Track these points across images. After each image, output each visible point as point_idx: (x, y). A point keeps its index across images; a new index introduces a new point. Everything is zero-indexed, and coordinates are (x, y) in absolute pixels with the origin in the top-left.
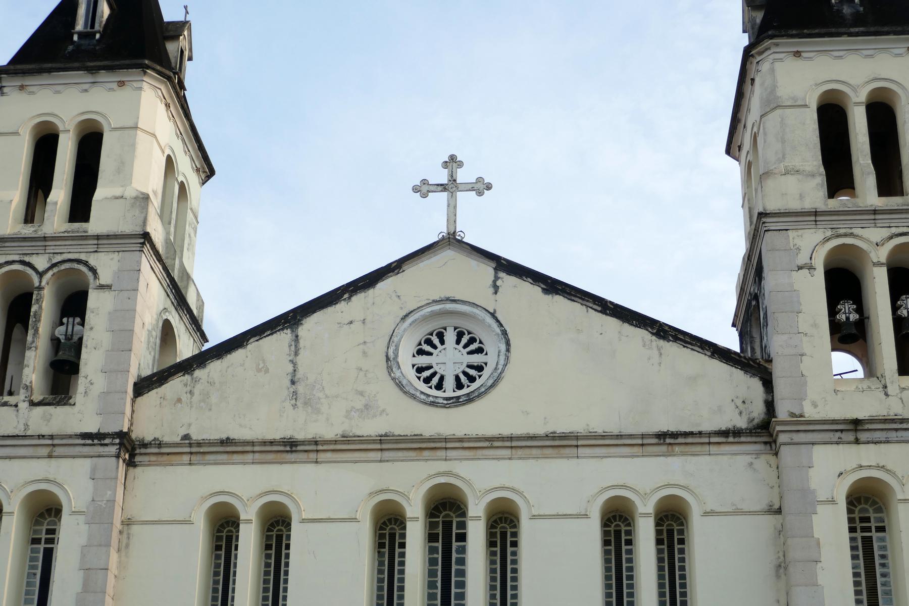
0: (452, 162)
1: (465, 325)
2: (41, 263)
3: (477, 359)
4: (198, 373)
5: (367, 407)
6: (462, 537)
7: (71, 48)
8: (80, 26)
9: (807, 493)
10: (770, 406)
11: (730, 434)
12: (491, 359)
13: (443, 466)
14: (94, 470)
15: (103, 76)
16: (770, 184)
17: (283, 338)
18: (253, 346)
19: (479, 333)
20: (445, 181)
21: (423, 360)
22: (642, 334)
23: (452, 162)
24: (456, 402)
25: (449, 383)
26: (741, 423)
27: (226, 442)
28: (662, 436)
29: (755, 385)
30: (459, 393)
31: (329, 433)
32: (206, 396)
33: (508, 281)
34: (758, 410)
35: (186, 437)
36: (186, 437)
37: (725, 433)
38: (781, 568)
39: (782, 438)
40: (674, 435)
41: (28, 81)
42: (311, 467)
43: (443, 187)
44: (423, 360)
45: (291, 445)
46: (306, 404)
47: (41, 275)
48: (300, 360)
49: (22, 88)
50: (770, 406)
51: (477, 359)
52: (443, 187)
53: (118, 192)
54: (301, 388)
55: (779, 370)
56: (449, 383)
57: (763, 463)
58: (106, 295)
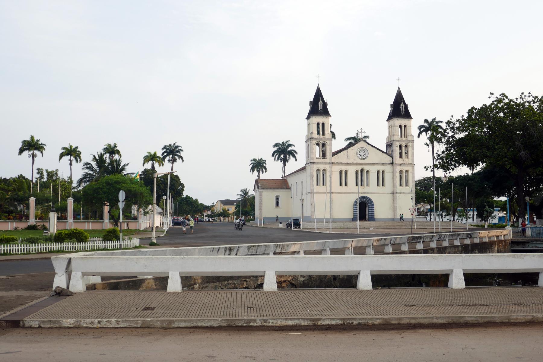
0: (361, 129)
1: (364, 150)
2: (321, 142)
3: (365, 154)
4: (338, 155)
5: (355, 160)
6: (363, 173)
7: (319, 111)
8: (320, 108)
9: (396, 171)
10: (393, 161)
11: (389, 164)
12: (366, 154)
13: (362, 166)
14: (330, 166)
15: (325, 117)
16: (394, 136)
17: (345, 152)
18: (343, 152)
19: (365, 151)
20: (361, 131)
21: (360, 154)
22: (381, 152)
23: (361, 129)
24: (363, 159)
25: (362, 157)
26: (390, 163)
27: (341, 163)
28: (383, 164)
29: (392, 158)
30: (364, 158)
31: (351, 162)
32: (338, 157)
33: (368, 145)
34: (392, 161)
35: (337, 162)
36: (337, 162)
37: (388, 164)
38: (393, 178)
39: (394, 165)
40: (384, 164)
41: (316, 117)
42: (350, 166)
43: (361, 132)
44: (360, 154)
45: (348, 163)
46: (349, 159)
47: (321, 143)
48: (348, 154)
49: (315, 117)
50: (393, 161)
51: (365, 154)
52: (361, 132)
53: (328, 133)
54: (348, 157)
55: (394, 158)
56: (362, 157)
57: (392, 167)
58: (328, 146)
